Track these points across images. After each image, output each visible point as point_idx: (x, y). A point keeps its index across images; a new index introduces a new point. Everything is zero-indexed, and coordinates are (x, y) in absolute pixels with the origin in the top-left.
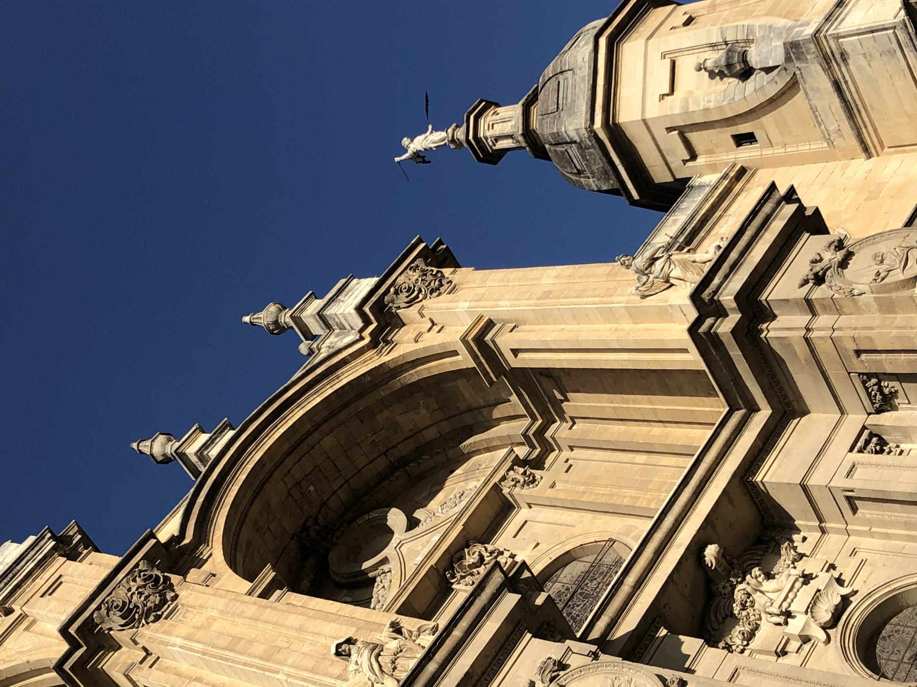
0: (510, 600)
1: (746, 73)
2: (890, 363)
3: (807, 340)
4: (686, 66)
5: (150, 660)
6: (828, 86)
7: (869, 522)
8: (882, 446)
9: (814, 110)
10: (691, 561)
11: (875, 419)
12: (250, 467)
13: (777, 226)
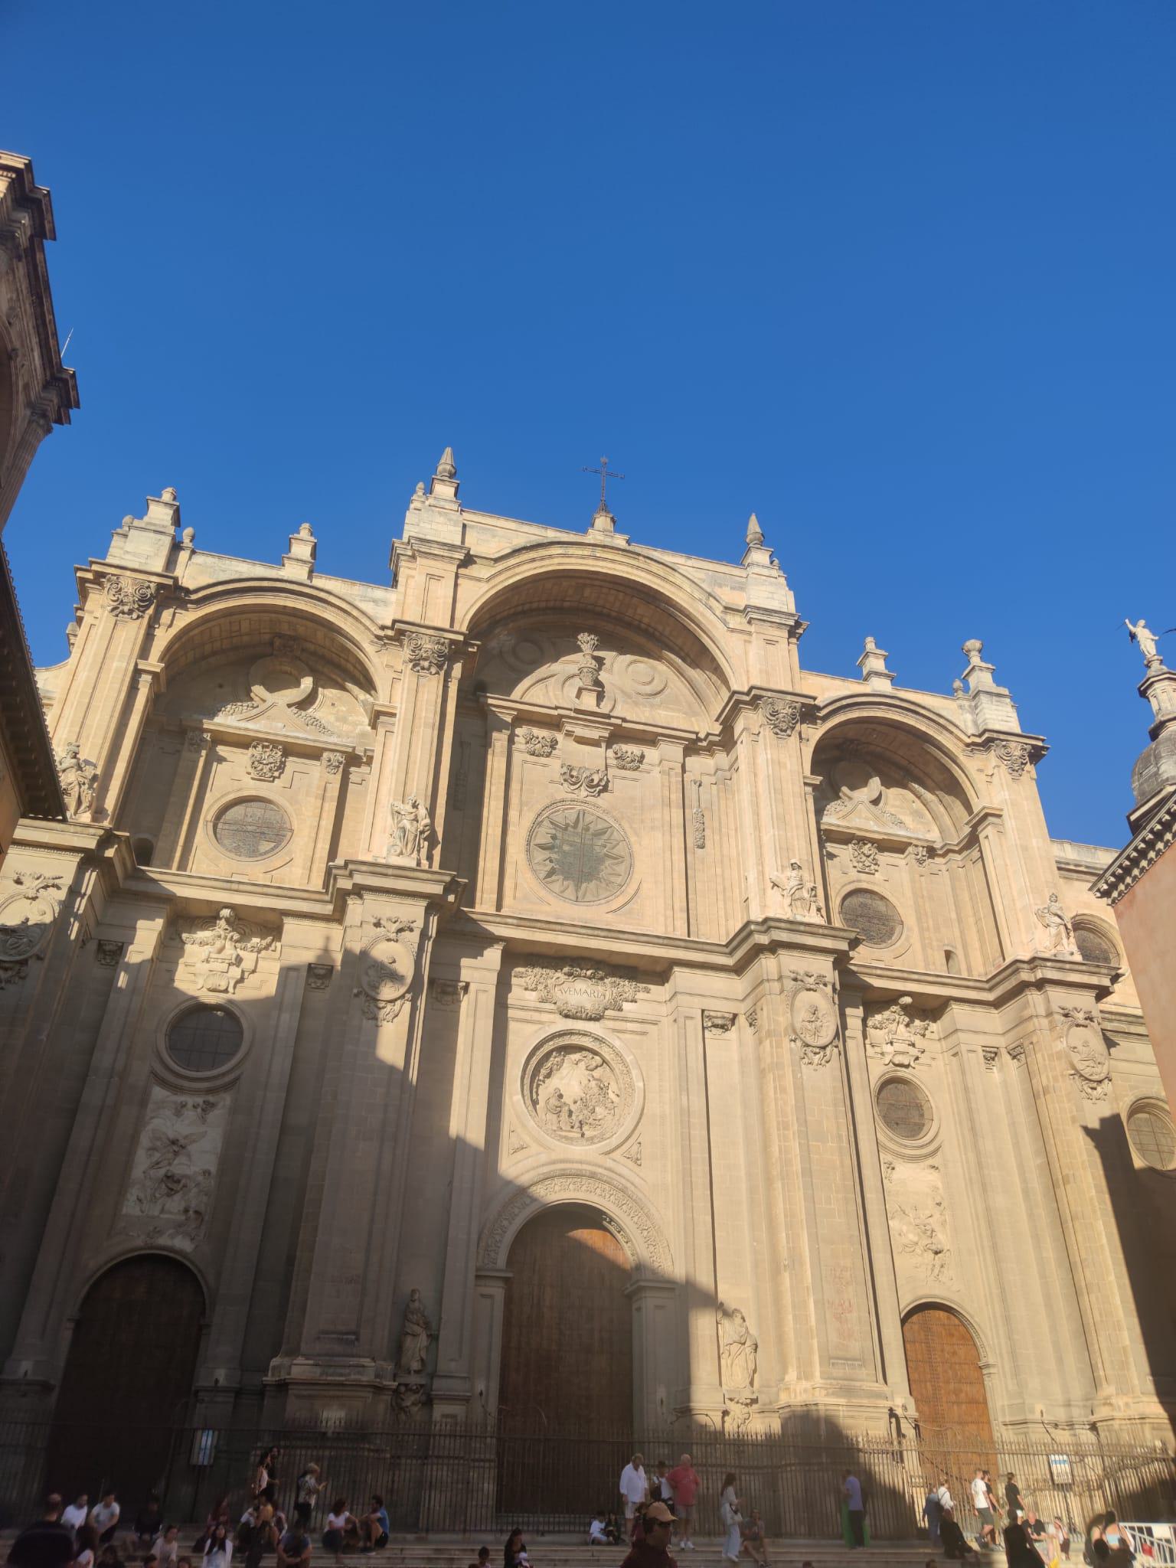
0: (844, 946)
5: (755, 738)
11: (1004, 1051)
12: (872, 714)
13: (1094, 980)
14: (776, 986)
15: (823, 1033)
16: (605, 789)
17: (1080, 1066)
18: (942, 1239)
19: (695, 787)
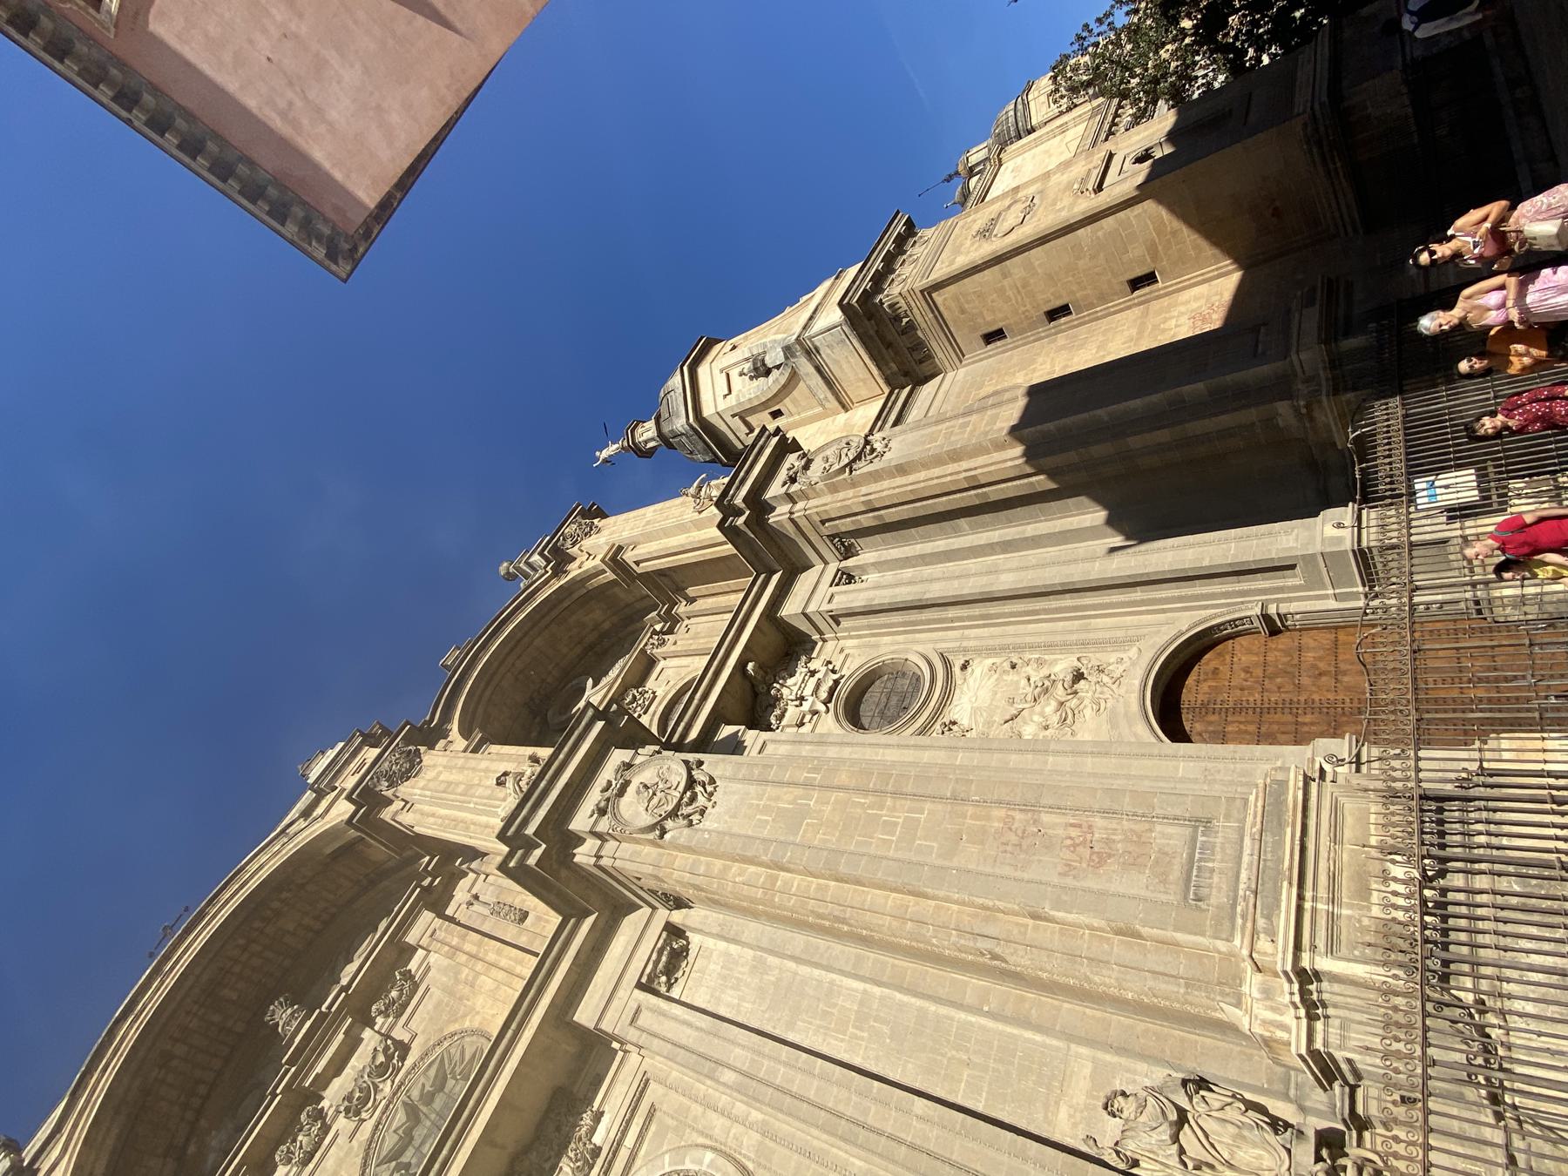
1: (768, 372)
2: (846, 525)
3: (792, 520)
4: (734, 373)
6: (812, 370)
7: (846, 630)
8: (850, 579)
9: (809, 387)
10: (738, 677)
11: (844, 564)
13: (768, 451)
14: (612, 844)
15: (674, 780)
16: (404, 1048)
17: (845, 461)
18: (1062, 666)
19: (477, 907)
